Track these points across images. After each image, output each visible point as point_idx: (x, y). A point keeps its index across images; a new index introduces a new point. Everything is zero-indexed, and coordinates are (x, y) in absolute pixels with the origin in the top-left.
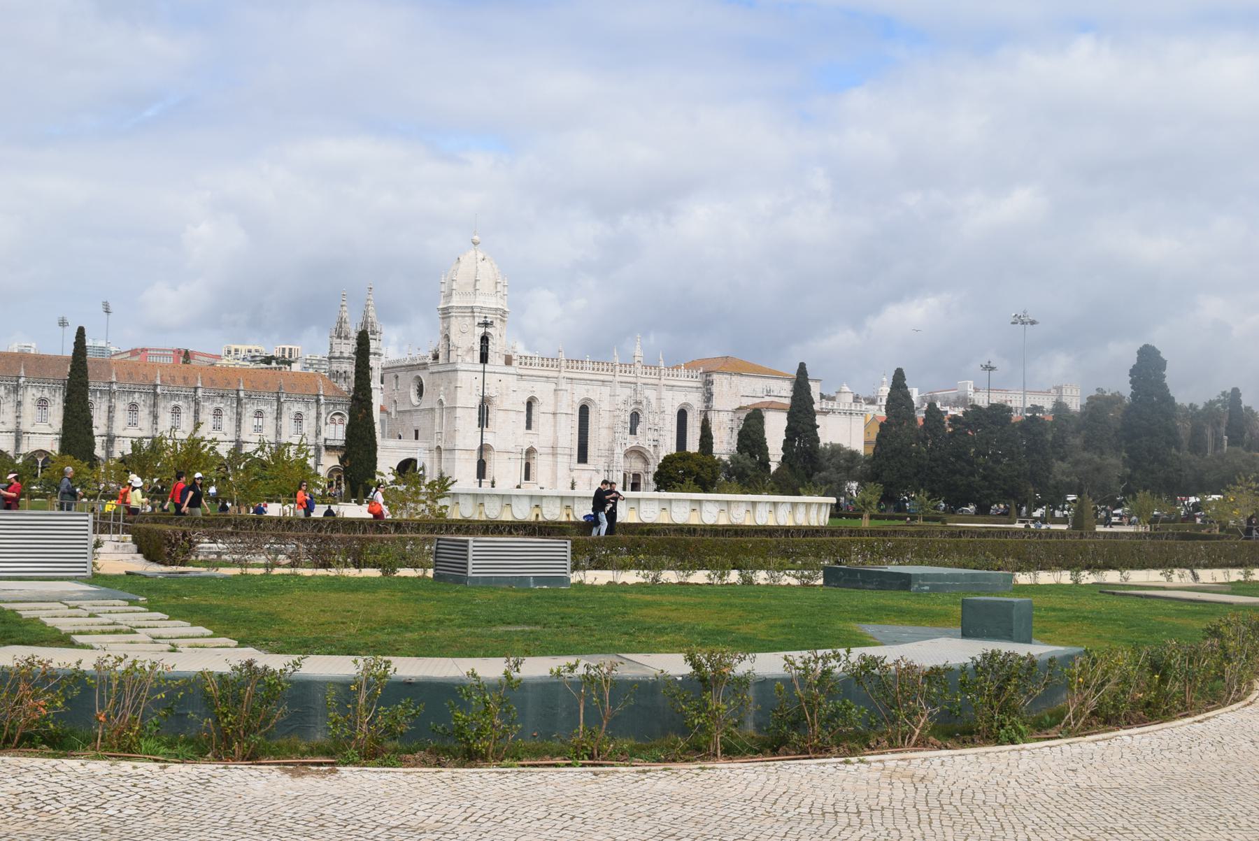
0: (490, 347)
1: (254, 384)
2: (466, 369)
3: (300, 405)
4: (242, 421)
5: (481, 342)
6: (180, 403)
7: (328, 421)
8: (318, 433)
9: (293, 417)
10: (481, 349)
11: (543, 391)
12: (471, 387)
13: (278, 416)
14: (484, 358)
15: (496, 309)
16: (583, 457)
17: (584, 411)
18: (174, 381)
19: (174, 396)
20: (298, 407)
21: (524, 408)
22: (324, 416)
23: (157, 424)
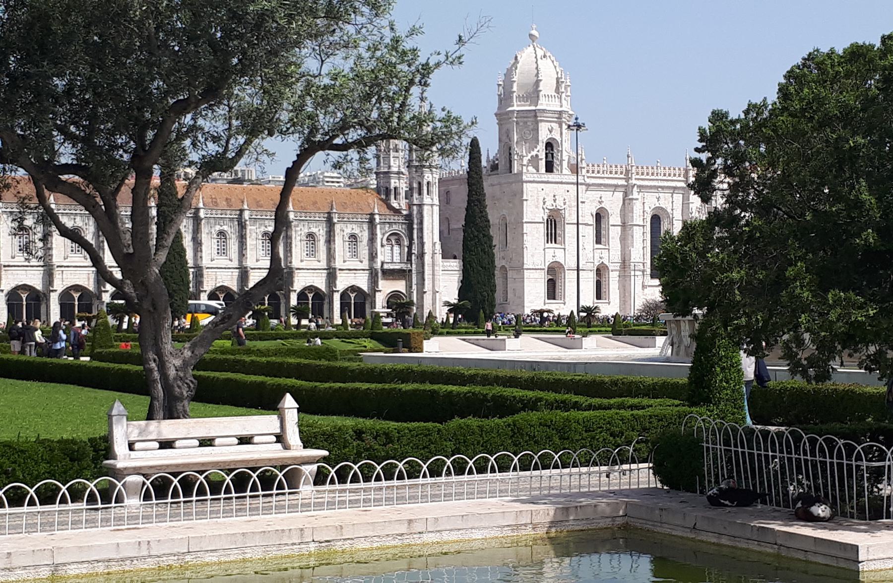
0: (555, 155)
1: (302, 204)
2: (532, 179)
3: (354, 226)
4: (293, 246)
5: (546, 150)
6: (225, 228)
7: (385, 242)
8: (373, 257)
9: (347, 239)
10: (546, 157)
11: (613, 203)
12: (538, 199)
13: (330, 240)
14: (549, 168)
15: (561, 113)
20: (349, 229)
21: (592, 221)
22: (379, 236)
23: (201, 251)
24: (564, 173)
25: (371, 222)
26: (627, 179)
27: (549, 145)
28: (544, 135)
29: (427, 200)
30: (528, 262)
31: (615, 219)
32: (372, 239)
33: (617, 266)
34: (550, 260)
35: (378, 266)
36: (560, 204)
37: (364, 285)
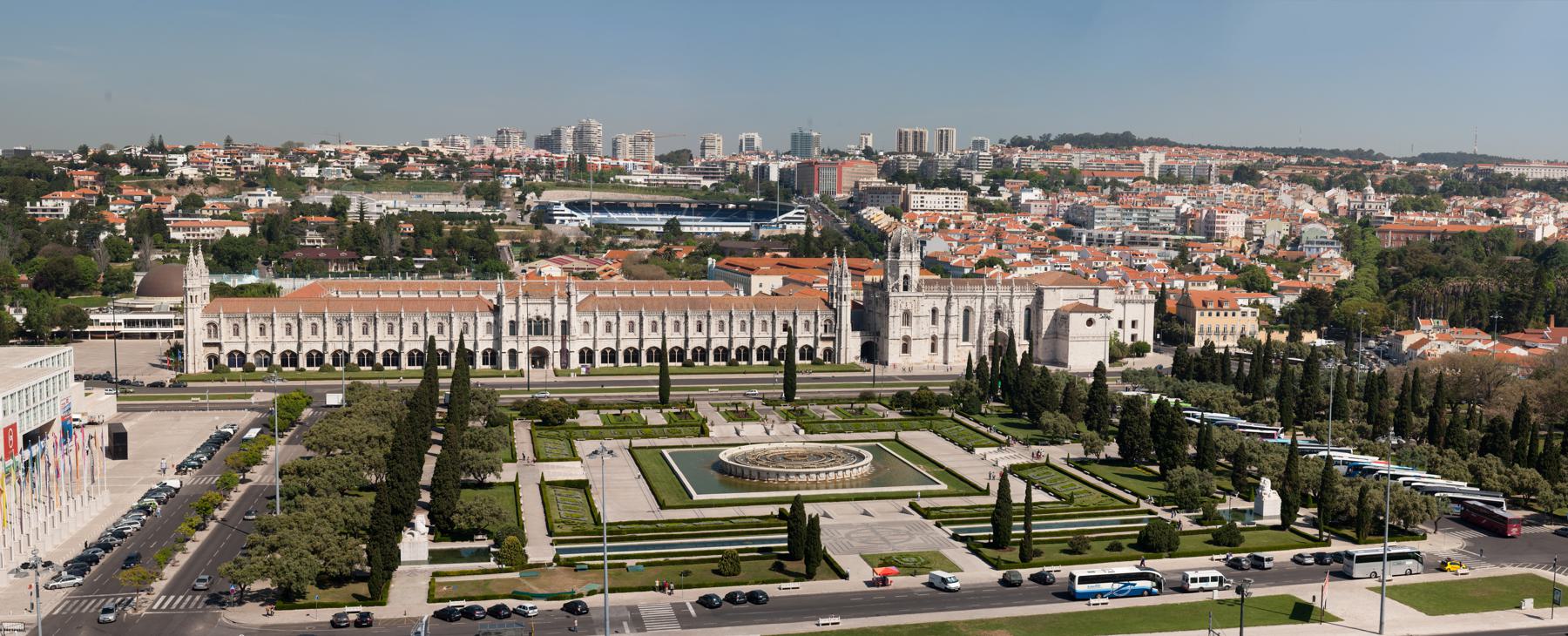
8: (816, 331)
14: (906, 289)
15: (911, 262)
16: (966, 338)
17: (967, 311)
18: (742, 307)
19: (740, 316)
24: (912, 292)
25: (816, 313)
26: (950, 292)
27: (906, 277)
28: (902, 273)
29: (844, 303)
30: (891, 336)
31: (942, 312)
32: (816, 322)
33: (943, 336)
34: (903, 334)
35: (819, 335)
36: (909, 307)
37: (812, 345)
